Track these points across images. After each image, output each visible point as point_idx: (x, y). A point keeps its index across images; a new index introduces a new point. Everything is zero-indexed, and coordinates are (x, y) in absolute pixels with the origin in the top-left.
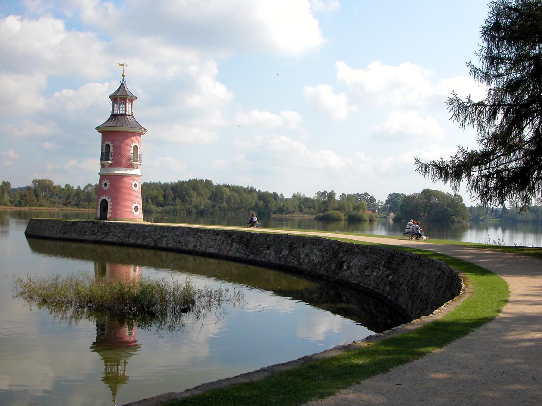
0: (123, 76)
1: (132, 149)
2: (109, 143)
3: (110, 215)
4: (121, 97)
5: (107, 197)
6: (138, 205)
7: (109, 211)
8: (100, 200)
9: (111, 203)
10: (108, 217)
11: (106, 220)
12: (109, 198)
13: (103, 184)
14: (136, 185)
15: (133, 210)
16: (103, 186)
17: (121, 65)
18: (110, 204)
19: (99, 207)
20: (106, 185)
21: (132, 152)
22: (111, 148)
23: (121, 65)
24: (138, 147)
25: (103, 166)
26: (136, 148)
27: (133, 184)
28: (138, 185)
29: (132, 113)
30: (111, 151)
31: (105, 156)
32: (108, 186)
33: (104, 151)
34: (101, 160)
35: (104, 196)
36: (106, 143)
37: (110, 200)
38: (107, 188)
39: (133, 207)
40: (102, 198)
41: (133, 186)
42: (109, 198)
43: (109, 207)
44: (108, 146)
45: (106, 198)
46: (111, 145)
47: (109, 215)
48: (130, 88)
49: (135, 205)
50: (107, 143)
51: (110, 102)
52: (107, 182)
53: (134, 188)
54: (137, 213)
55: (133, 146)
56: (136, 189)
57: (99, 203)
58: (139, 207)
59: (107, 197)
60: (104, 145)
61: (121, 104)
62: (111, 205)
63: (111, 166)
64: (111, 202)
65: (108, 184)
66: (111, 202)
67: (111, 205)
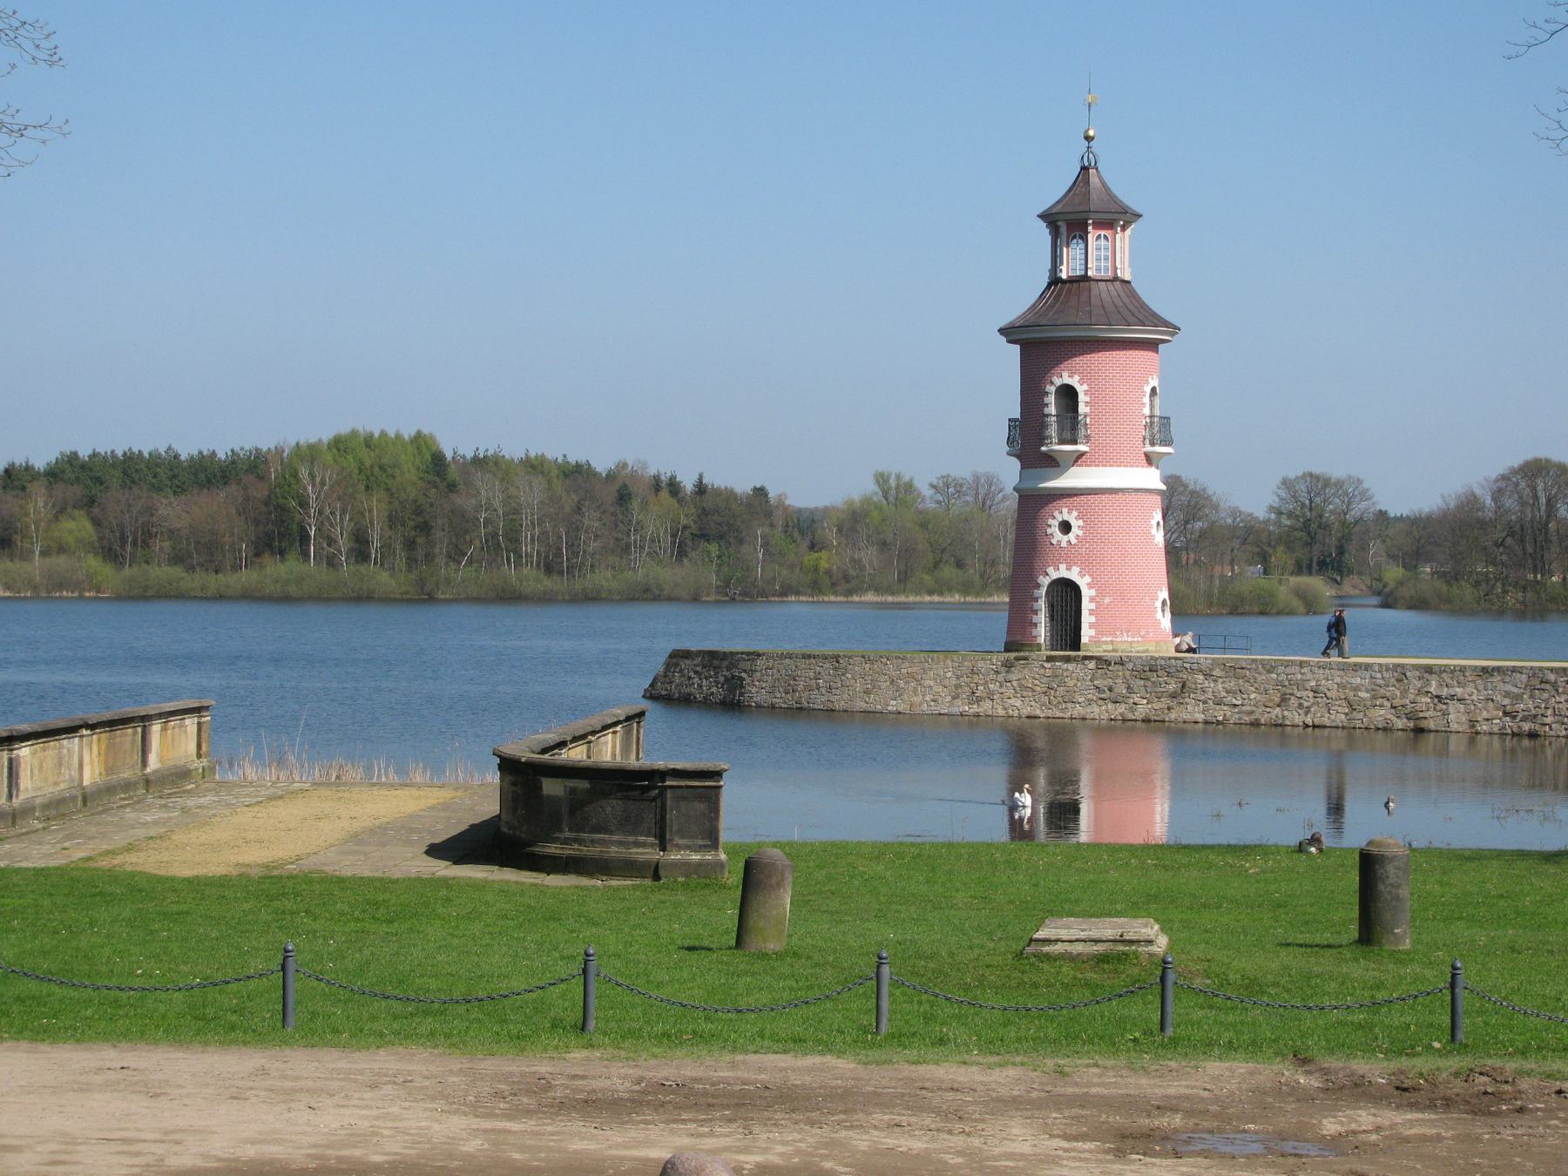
0: (1088, 138)
3: (1092, 632)
7: (1086, 619)
8: (1045, 582)
9: (1093, 592)
10: (1084, 640)
12: (1081, 574)
18: (1086, 593)
19: (1042, 604)
20: (1066, 527)
22: (1082, 398)
30: (1082, 409)
37: (1088, 579)
38: (1071, 536)
43: (1086, 605)
45: (1073, 575)
46: (1081, 389)
47: (1086, 634)
48: (1120, 180)
51: (1043, 232)
62: (1092, 600)
64: (1090, 586)
65: (1075, 524)
66: (1090, 586)
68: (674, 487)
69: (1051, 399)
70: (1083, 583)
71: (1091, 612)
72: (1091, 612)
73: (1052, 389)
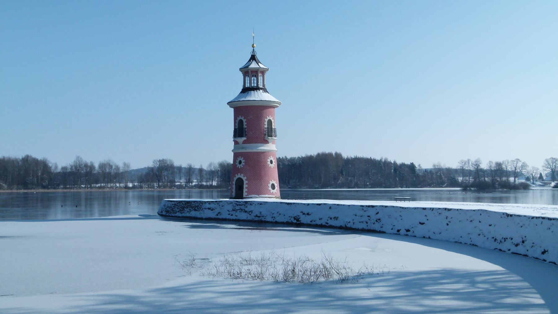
1: (266, 123)
2: (242, 118)
5: (242, 175)
6: (274, 182)
8: (235, 179)
9: (247, 182)
10: (244, 196)
11: (242, 199)
12: (244, 176)
13: (238, 161)
14: (271, 162)
15: (270, 188)
16: (237, 163)
18: (245, 182)
19: (234, 186)
21: (266, 126)
22: (245, 123)
24: (273, 121)
25: (236, 143)
26: (270, 122)
27: (269, 160)
28: (273, 161)
29: (264, 85)
30: (245, 126)
31: (239, 132)
32: (243, 163)
33: (237, 127)
34: (235, 136)
35: (239, 174)
37: (245, 178)
38: (241, 165)
39: (270, 185)
41: (269, 163)
42: (244, 176)
43: (245, 186)
44: (241, 122)
45: (242, 176)
46: (244, 121)
47: (245, 194)
49: (271, 183)
50: (240, 118)
52: (242, 159)
53: (270, 165)
54: (275, 191)
55: (267, 120)
56: (272, 166)
57: (234, 183)
58: (276, 185)
59: (242, 175)
60: (237, 121)
61: (253, 76)
64: (246, 180)
65: (243, 161)
66: (246, 180)
67: (246, 184)
70: (244, 179)
71: (246, 188)
72: (246, 188)
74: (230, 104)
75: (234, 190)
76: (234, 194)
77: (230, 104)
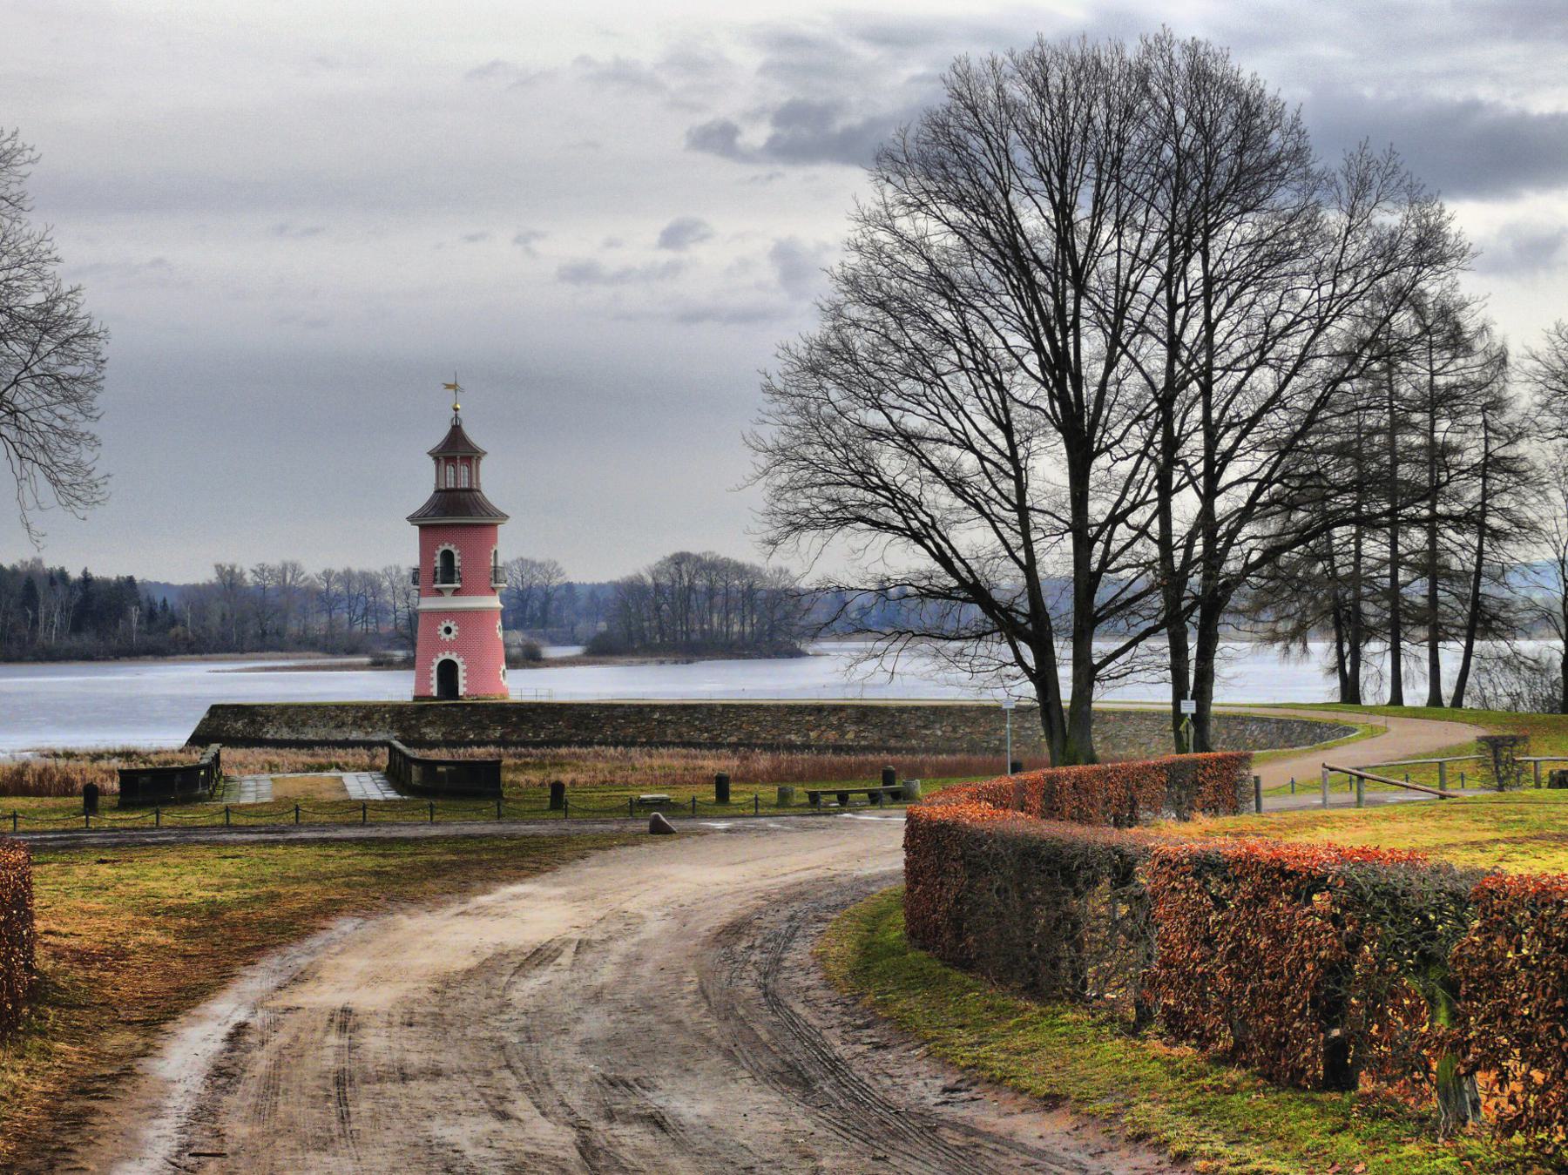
2: (452, 548)
4: (456, 449)
7: (462, 682)
8: (437, 662)
17: (449, 387)
18: (461, 667)
19: (434, 675)
20: (448, 630)
22: (457, 558)
23: (449, 387)
30: (457, 564)
36: (442, 548)
40: (442, 657)
43: (461, 674)
44: (448, 556)
45: (453, 657)
46: (456, 552)
52: (452, 625)
57: (434, 668)
63: (456, 592)
68: (63, 575)
69: (438, 558)
70: (459, 661)
73: (438, 553)
74: (411, 519)
75: (434, 682)
76: (434, 691)
77: (411, 519)
